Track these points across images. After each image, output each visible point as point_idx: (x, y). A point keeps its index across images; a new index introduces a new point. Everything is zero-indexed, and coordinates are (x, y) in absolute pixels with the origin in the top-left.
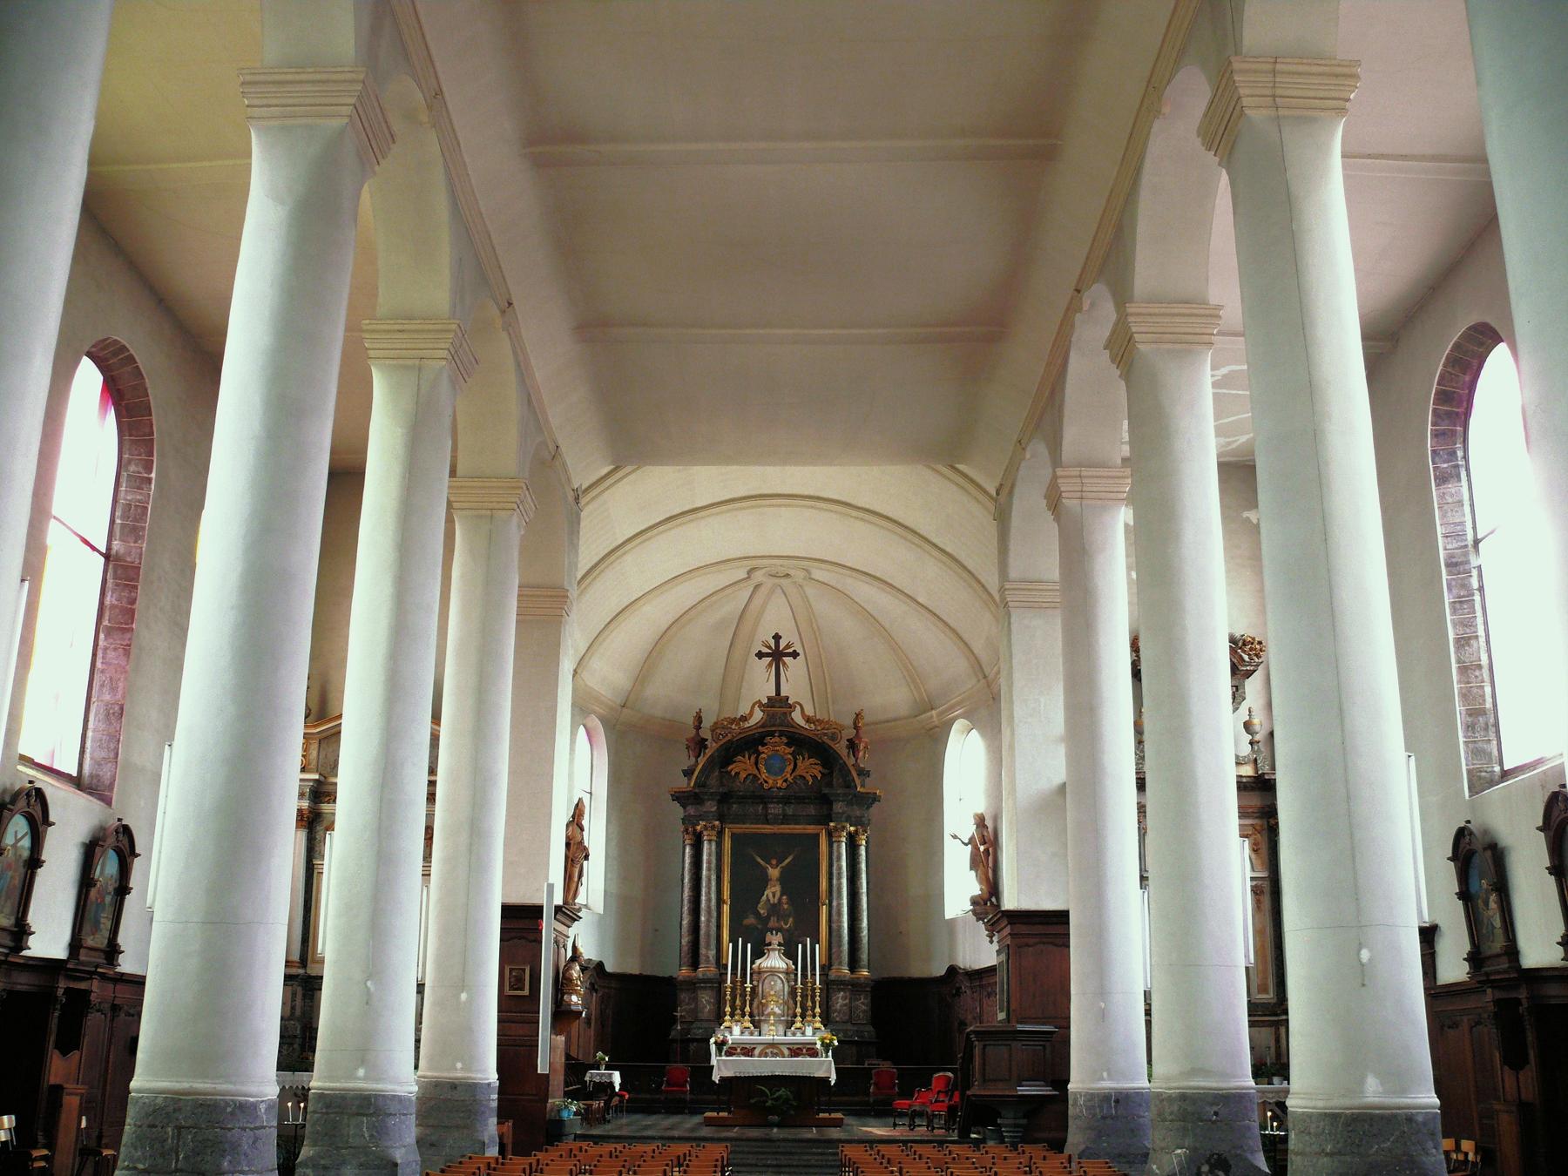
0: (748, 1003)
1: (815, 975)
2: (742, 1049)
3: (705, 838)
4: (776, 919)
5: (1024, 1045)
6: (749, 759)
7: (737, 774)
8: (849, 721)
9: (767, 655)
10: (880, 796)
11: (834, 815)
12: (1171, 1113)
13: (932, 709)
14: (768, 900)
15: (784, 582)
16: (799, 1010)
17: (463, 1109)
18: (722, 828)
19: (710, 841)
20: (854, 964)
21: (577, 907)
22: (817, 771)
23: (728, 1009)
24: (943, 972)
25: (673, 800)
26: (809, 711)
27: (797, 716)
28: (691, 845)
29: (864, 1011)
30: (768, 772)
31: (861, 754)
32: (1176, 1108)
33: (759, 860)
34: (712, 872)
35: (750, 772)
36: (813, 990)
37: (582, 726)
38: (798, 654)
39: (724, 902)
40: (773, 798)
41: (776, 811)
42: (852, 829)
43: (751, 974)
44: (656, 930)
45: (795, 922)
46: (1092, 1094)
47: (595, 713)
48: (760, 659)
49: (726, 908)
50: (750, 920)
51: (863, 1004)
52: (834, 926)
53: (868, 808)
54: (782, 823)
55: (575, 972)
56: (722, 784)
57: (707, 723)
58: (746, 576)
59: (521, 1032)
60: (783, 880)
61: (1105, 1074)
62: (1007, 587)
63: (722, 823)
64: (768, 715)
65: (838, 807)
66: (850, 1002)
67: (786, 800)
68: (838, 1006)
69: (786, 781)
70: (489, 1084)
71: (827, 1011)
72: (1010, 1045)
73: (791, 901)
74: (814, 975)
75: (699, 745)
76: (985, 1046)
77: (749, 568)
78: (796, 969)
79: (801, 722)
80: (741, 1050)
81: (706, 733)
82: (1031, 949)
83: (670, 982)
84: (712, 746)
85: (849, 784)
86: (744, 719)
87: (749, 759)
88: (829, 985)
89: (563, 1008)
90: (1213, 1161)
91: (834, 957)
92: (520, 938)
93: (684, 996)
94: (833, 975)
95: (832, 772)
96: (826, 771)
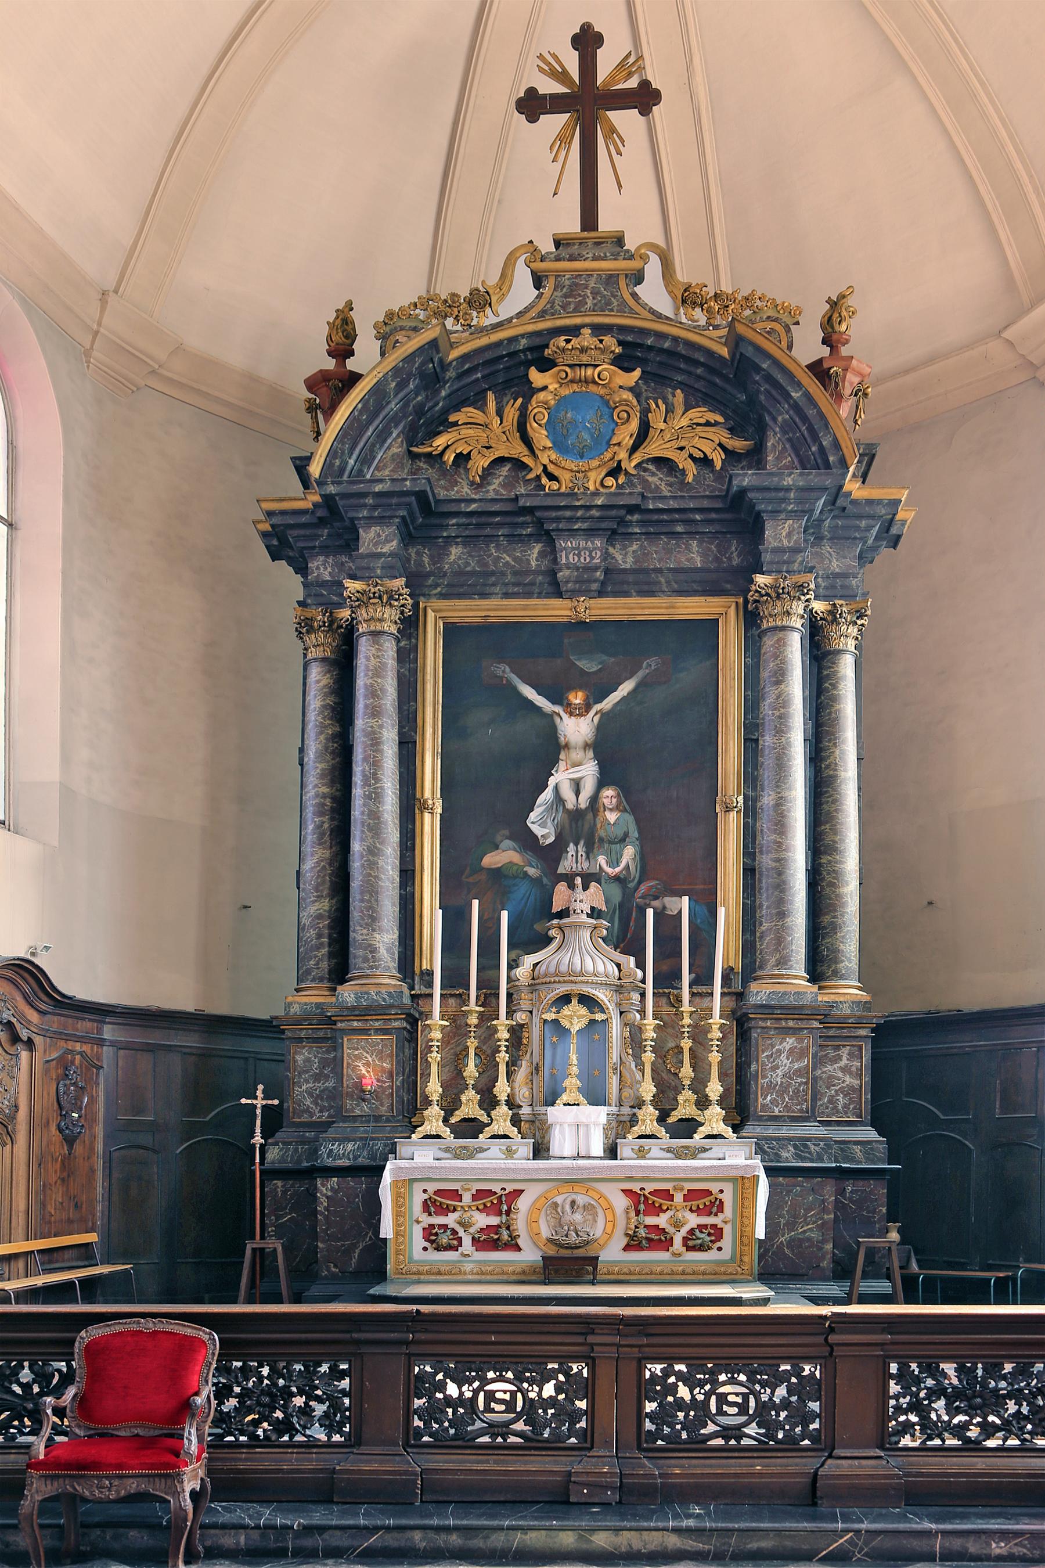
0: (502, 1069)
2: (479, 1195)
4: (581, 850)
6: (500, 413)
7: (462, 459)
9: (555, 104)
11: (766, 557)
14: (559, 799)
16: (648, 1090)
23: (434, 1088)
30: (559, 445)
33: (529, 692)
36: (699, 1034)
40: (571, 520)
41: (585, 559)
45: (643, 857)
48: (532, 119)
49: (430, 826)
54: (601, 594)
63: (417, 584)
68: (778, 1077)
69: (615, 472)
73: (630, 802)
78: (643, 981)
80: (474, 1198)
86: (480, 300)
87: (500, 413)
91: (765, 945)
96: (738, 444)
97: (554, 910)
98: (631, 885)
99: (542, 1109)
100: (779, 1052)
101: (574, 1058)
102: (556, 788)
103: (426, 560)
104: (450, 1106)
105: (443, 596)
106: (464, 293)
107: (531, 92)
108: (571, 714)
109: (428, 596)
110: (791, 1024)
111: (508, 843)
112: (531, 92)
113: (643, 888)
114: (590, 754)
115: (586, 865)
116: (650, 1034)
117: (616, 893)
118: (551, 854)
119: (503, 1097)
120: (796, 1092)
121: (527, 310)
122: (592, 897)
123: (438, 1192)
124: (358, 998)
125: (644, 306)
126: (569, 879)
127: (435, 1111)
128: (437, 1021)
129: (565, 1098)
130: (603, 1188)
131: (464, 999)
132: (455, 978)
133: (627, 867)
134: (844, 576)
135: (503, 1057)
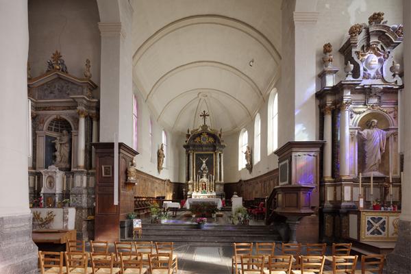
8: (219, 130)
15: (206, 98)
24: (238, 181)
27: (209, 129)
50: (199, 171)
51: (222, 188)
57: (190, 130)
65: (217, 148)
75: (188, 136)
81: (190, 133)
85: (219, 143)
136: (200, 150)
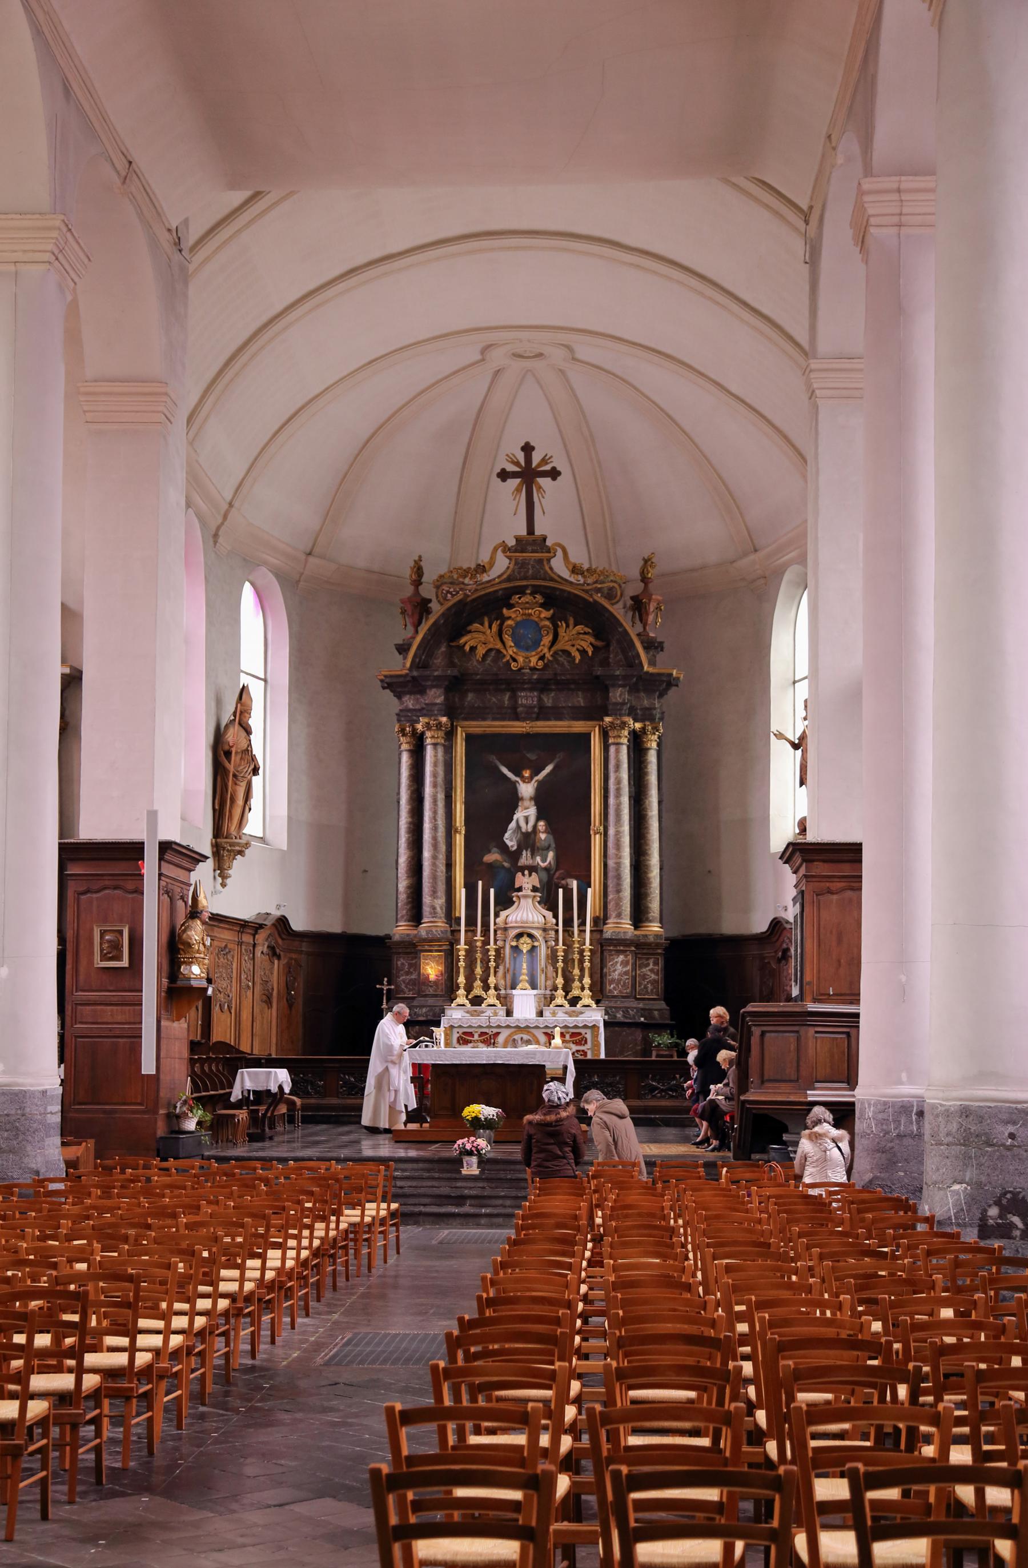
0: (492, 971)
1: (585, 931)
2: (482, 1034)
3: (428, 741)
4: (529, 855)
5: (817, 1032)
6: (490, 627)
7: (473, 649)
8: (635, 573)
9: (514, 475)
10: (678, 678)
11: (610, 707)
12: (948, 1135)
13: (756, 551)
14: (518, 827)
16: (560, 981)
17: (8, 1126)
18: (452, 724)
19: (435, 745)
20: (639, 916)
21: (243, 841)
22: (587, 643)
23: (461, 980)
25: (384, 688)
26: (579, 556)
27: (558, 566)
28: (409, 751)
29: (654, 982)
30: (517, 645)
31: (651, 618)
32: (954, 1127)
33: (505, 770)
34: (439, 789)
35: (490, 646)
36: (581, 952)
37: (247, 586)
38: (559, 473)
39: (456, 831)
41: (530, 702)
42: (638, 726)
43: (495, 931)
44: (365, 871)
45: (558, 858)
46: (885, 1103)
47: (265, 563)
48: (504, 480)
50: (493, 857)
51: (652, 972)
52: (611, 863)
53: (661, 696)
54: (537, 719)
55: (196, 933)
56: (451, 664)
57: (430, 576)
58: (479, 357)
59: (119, 1018)
60: (539, 799)
61: (904, 1076)
62: (813, 366)
64: (516, 563)
65: (618, 695)
66: (634, 969)
67: (542, 686)
68: (616, 975)
69: (542, 658)
70: (44, 1093)
71: (602, 983)
72: (797, 1032)
73: (551, 829)
74: (582, 932)
75: (421, 607)
76: (763, 1033)
77: (484, 344)
78: (557, 924)
79: (565, 574)
80: (480, 1036)
81: (427, 591)
82: (835, 897)
83: (382, 942)
84: (437, 609)
86: (481, 569)
87: (490, 627)
88: (604, 946)
89: (180, 983)
90: (1004, 1202)
92: (116, 888)
93: (401, 962)
94: (609, 930)
95: (608, 645)
96: (599, 644)
97: (517, 886)
98: (552, 872)
99: (509, 991)
100: (617, 962)
101: (525, 966)
102: (517, 821)
103: (457, 700)
104: (469, 989)
105: (466, 719)
106: (473, 566)
107: (503, 471)
108: (524, 782)
109: (458, 719)
110: (622, 948)
111: (495, 850)
112: (503, 471)
113: (557, 874)
114: (533, 803)
115: (531, 862)
116: (561, 953)
117: (544, 876)
118: (515, 856)
119: (492, 985)
120: (624, 983)
121: (502, 574)
122: (534, 880)
123: (464, 1033)
124: (427, 933)
125: (555, 573)
126: (522, 869)
127: (461, 992)
128: (462, 946)
129: (520, 986)
130: (535, 1032)
131: (474, 932)
132: (471, 921)
133: (550, 863)
134: (650, 709)
135: (492, 964)
136: (501, 715)
